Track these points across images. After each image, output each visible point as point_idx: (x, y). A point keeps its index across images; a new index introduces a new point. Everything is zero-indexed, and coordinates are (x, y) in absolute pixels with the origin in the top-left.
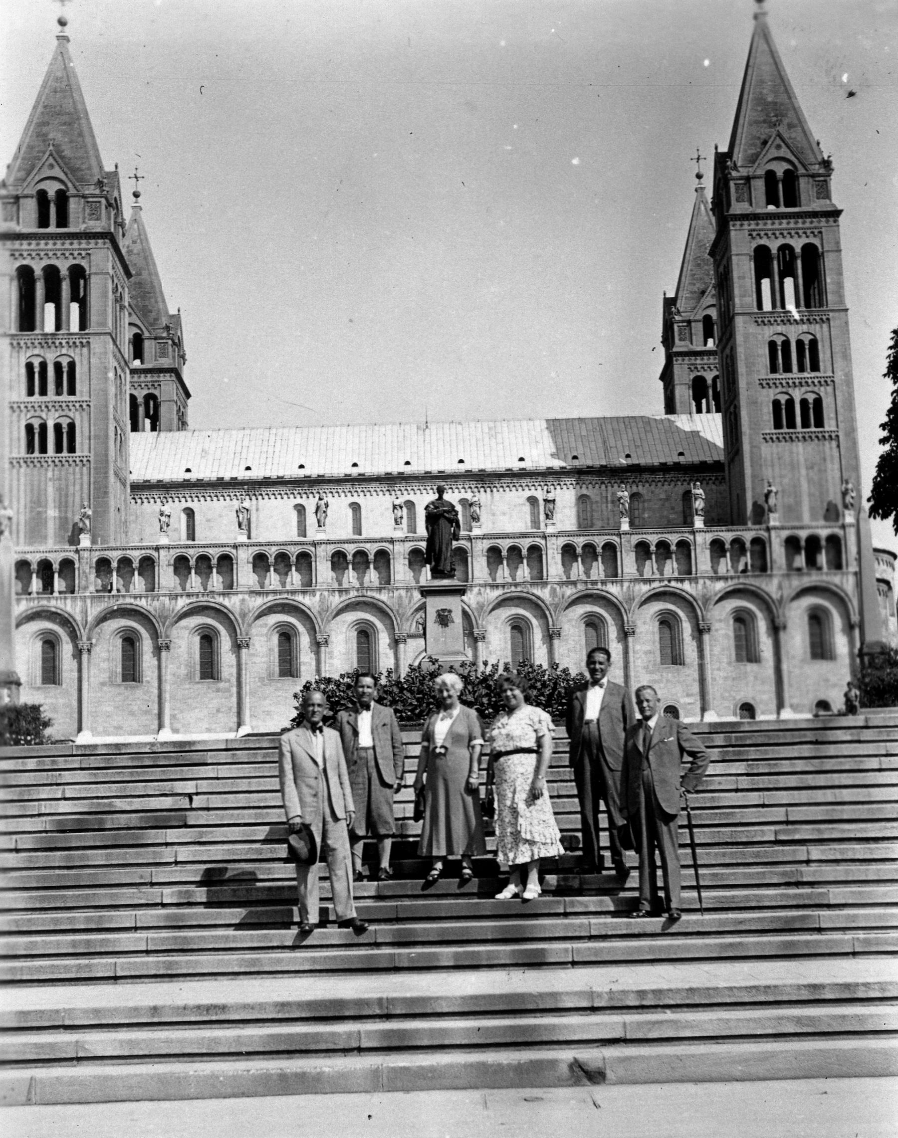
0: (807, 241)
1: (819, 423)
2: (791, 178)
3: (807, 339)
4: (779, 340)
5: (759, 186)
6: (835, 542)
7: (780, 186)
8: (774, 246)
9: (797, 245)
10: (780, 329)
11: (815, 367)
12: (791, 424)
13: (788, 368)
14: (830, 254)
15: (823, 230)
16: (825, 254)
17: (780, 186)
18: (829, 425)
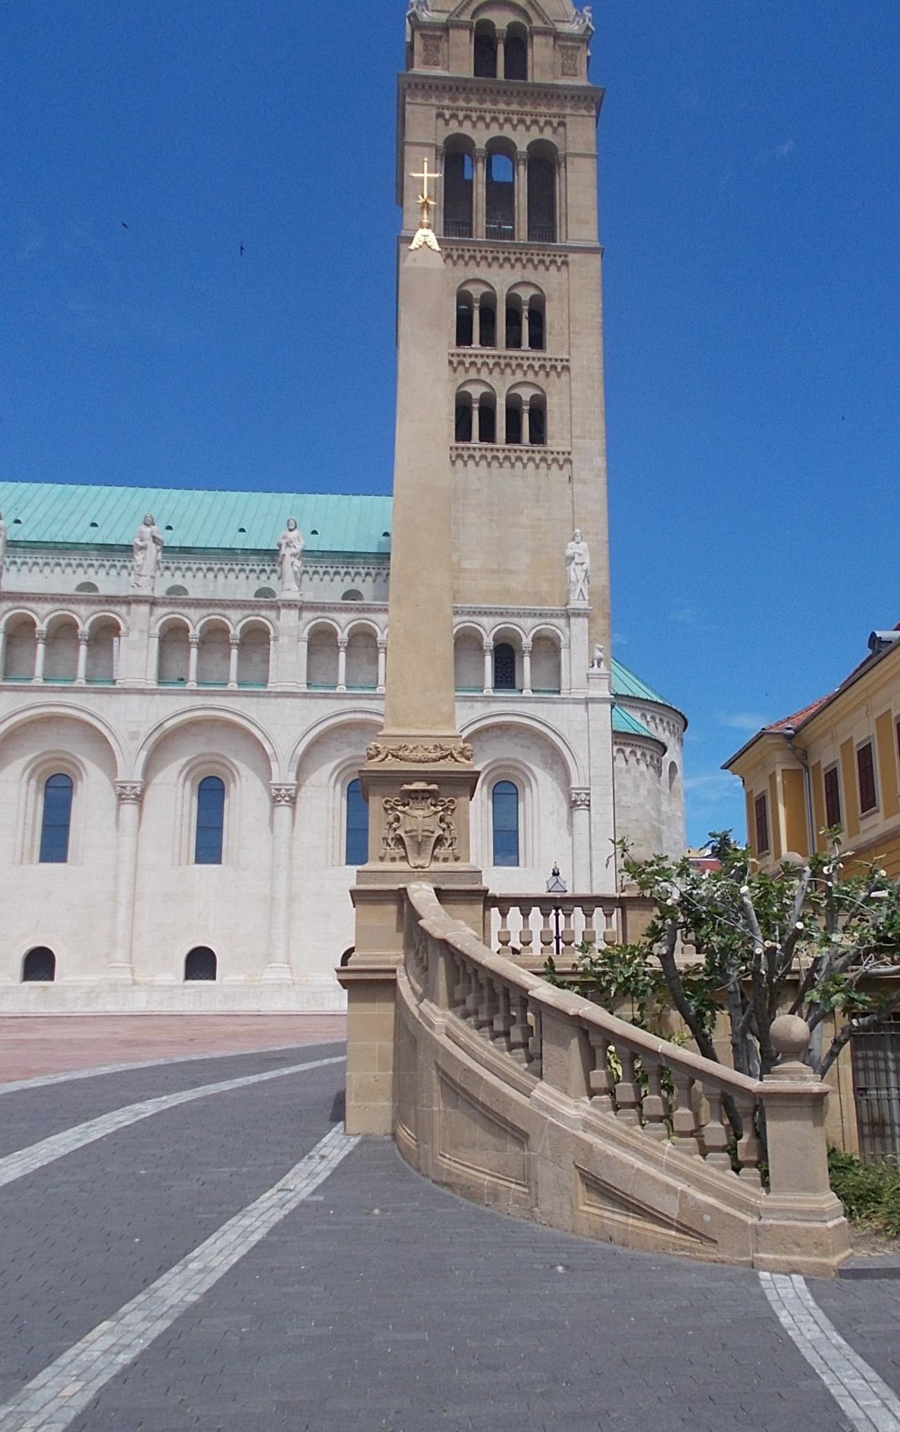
0: (541, 137)
1: (538, 436)
2: (518, 41)
3: (525, 294)
4: (476, 291)
5: (462, 46)
6: (548, 646)
7: (501, 48)
8: (481, 137)
9: (522, 140)
10: (482, 272)
11: (537, 342)
12: (488, 434)
13: (488, 339)
14: (576, 160)
15: (567, 120)
16: (569, 159)
17: (501, 48)
18: (556, 438)
